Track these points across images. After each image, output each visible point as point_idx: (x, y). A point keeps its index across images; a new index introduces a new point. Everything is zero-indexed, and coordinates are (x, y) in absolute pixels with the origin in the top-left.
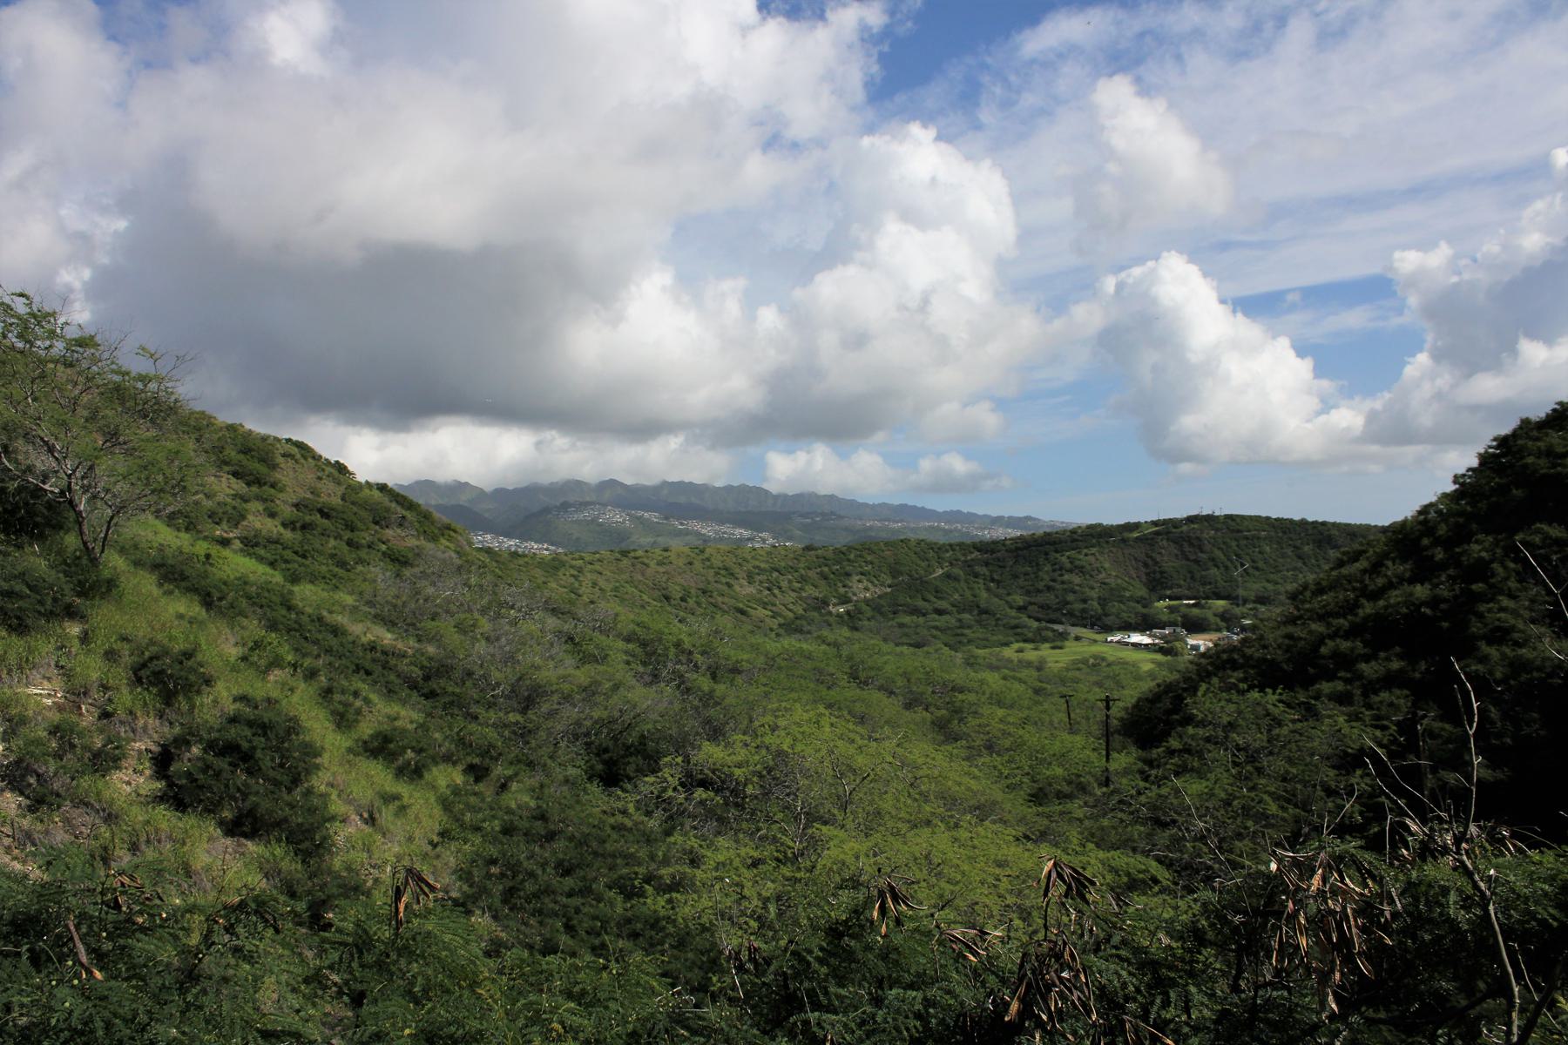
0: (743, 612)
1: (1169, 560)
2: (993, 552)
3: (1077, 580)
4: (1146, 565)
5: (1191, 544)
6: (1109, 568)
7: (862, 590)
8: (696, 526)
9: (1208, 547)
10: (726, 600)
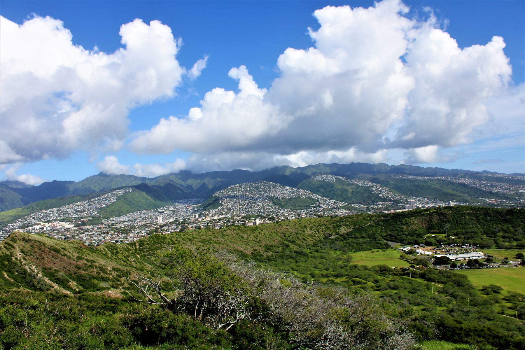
0: (304, 239)
1: (435, 220)
2: (387, 217)
3: (405, 227)
4: (428, 222)
5: (443, 216)
6: (416, 224)
7: (343, 230)
9: (448, 216)
10: (301, 236)
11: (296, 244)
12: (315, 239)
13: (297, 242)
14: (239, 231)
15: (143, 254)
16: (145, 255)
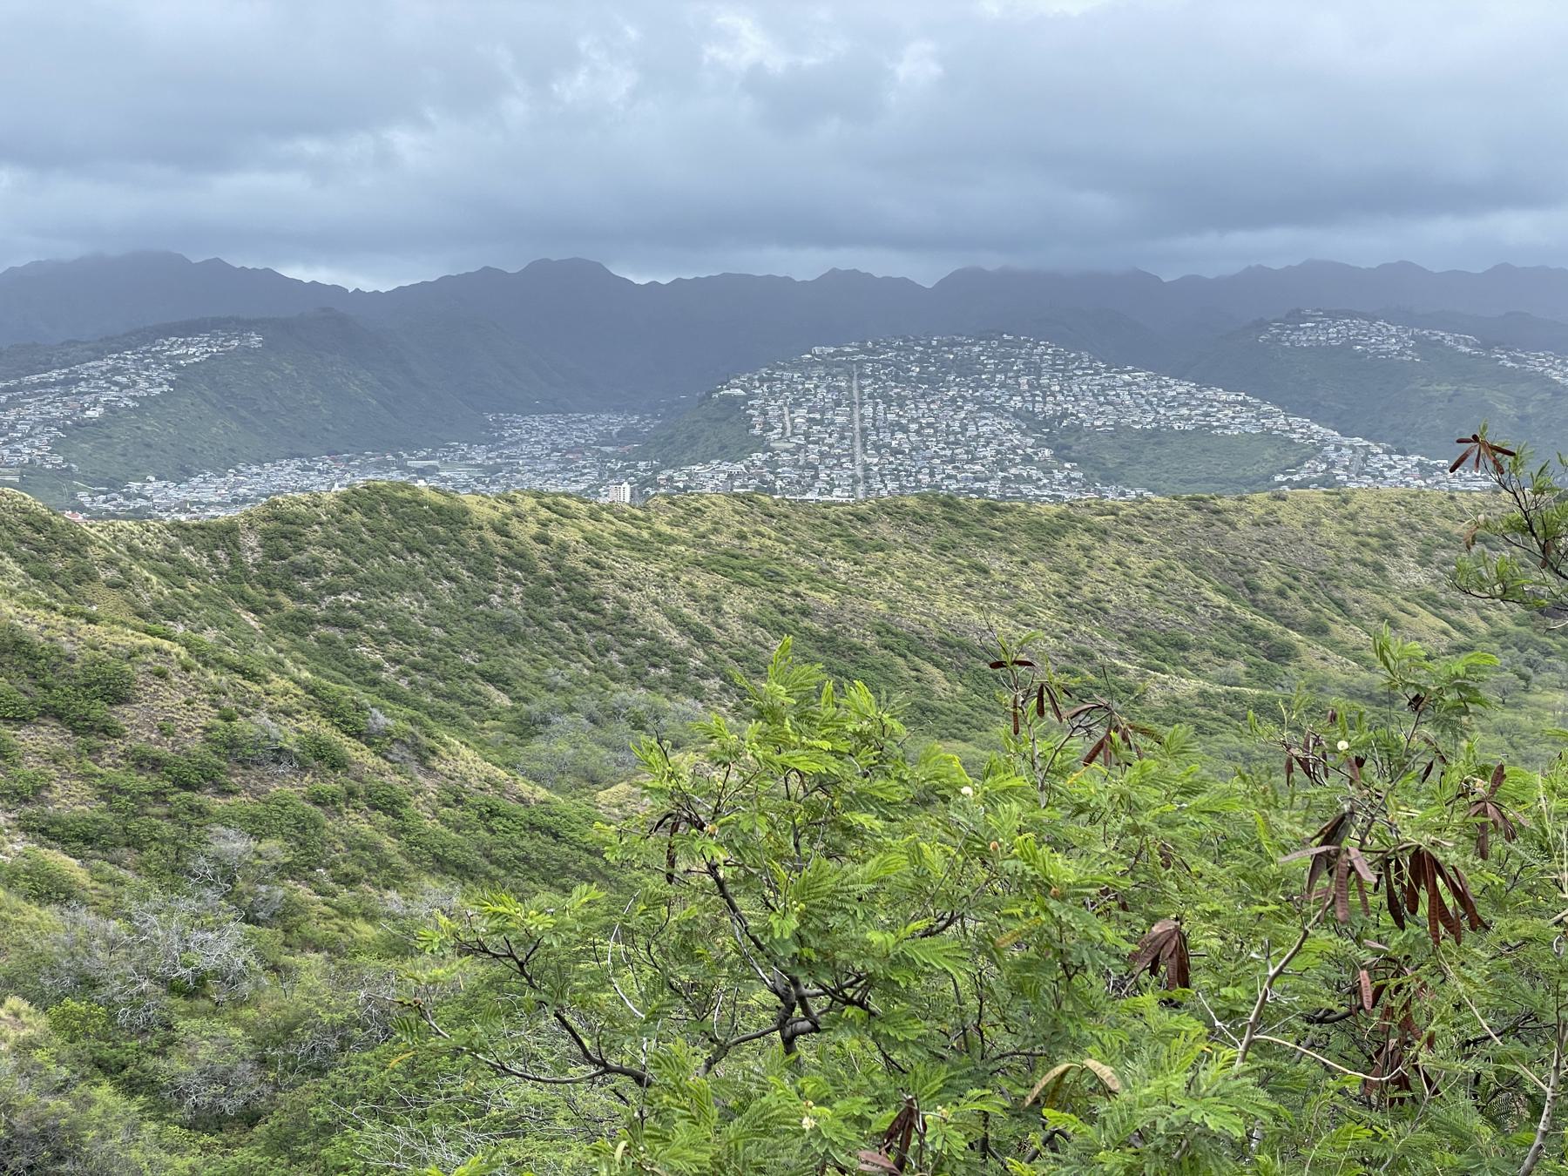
11: (1334, 645)
12: (1461, 628)
13: (1338, 630)
14: (954, 534)
15: (290, 605)
16: (311, 621)
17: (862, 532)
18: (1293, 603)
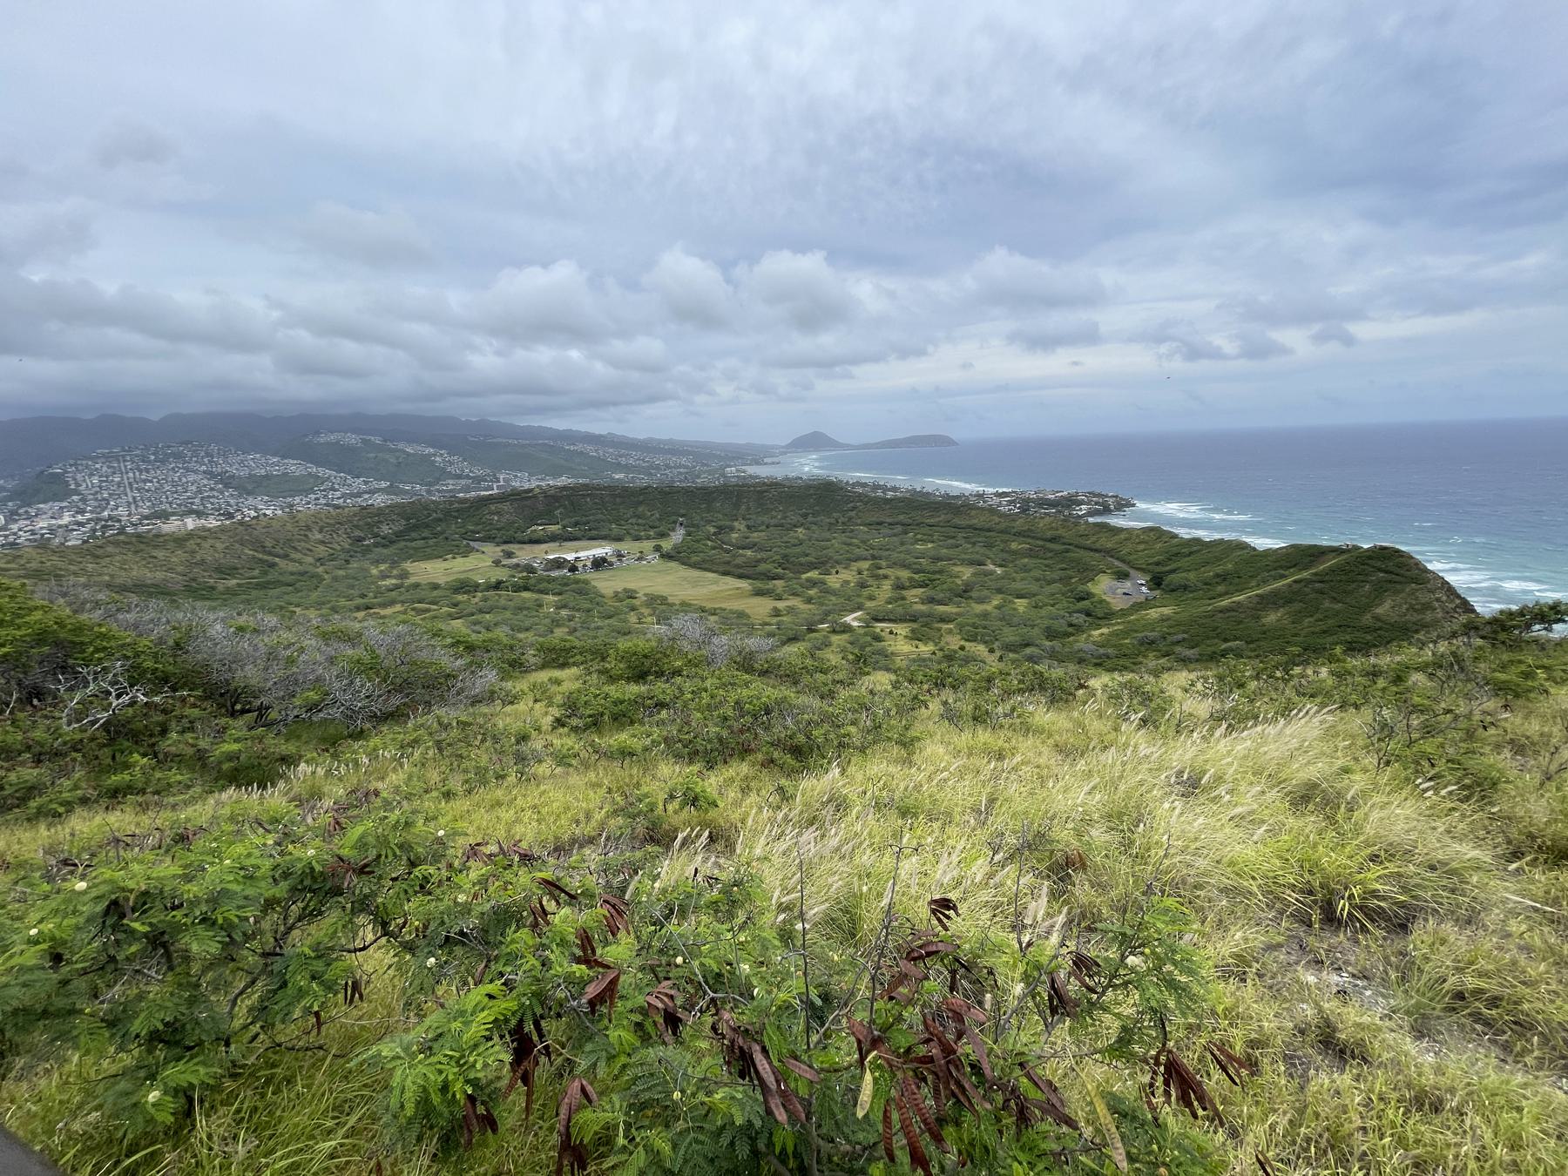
8: (401, 446)
17: (100, 552)
18: (278, 550)
